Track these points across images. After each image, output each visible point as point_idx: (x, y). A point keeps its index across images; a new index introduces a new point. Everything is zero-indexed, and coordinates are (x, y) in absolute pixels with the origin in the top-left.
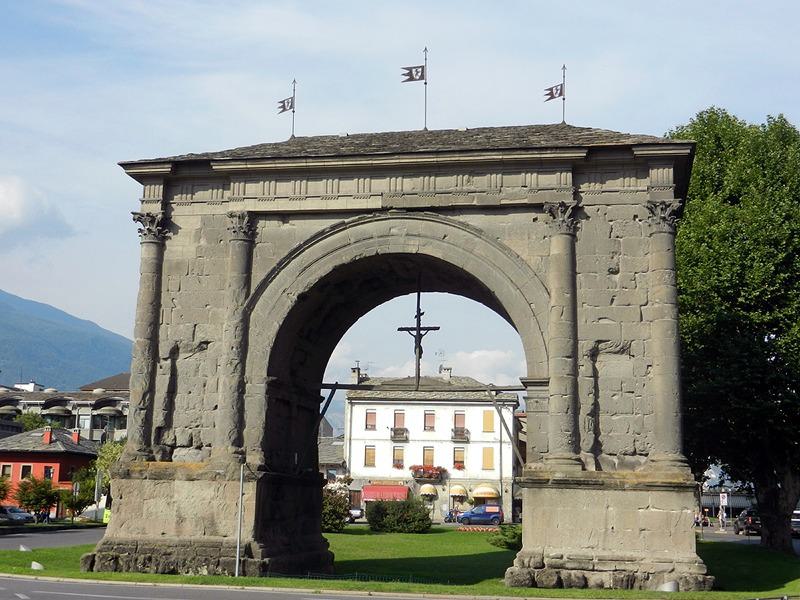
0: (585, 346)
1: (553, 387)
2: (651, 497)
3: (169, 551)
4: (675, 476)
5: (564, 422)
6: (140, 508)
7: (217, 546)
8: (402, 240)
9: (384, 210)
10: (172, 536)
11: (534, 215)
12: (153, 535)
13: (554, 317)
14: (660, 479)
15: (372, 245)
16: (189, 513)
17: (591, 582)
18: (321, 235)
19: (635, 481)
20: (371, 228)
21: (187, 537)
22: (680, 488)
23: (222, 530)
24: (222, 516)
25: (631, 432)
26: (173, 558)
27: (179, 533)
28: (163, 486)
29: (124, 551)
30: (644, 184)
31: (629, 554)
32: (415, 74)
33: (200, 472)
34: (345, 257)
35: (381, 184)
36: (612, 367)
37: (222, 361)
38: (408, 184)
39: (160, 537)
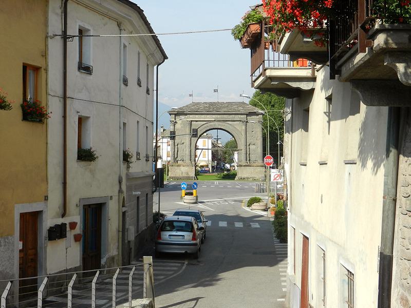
0: (248, 144)
5: (245, 156)
10: (181, 175)
12: (178, 175)
13: (243, 139)
16: (183, 171)
20: (212, 123)
28: (179, 168)
30: (258, 117)
32: (216, 91)
35: (214, 116)
36: (252, 147)
37: (187, 146)
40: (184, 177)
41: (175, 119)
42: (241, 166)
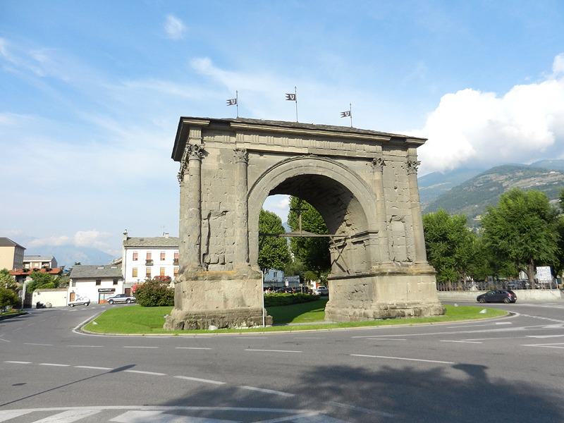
1: (381, 234)
2: (422, 277)
6: (204, 295)
7: (247, 311)
8: (315, 168)
9: (308, 154)
10: (222, 308)
11: (366, 162)
12: (212, 308)
14: (425, 271)
15: (302, 170)
16: (230, 296)
17: (406, 314)
18: (280, 163)
19: (416, 272)
20: (301, 162)
21: (230, 308)
23: (248, 304)
24: (247, 296)
26: (226, 319)
28: (215, 283)
29: (199, 318)
31: (416, 301)
34: (291, 175)
38: (317, 143)
39: (216, 309)
40: (231, 312)
41: (202, 142)
42: (383, 274)
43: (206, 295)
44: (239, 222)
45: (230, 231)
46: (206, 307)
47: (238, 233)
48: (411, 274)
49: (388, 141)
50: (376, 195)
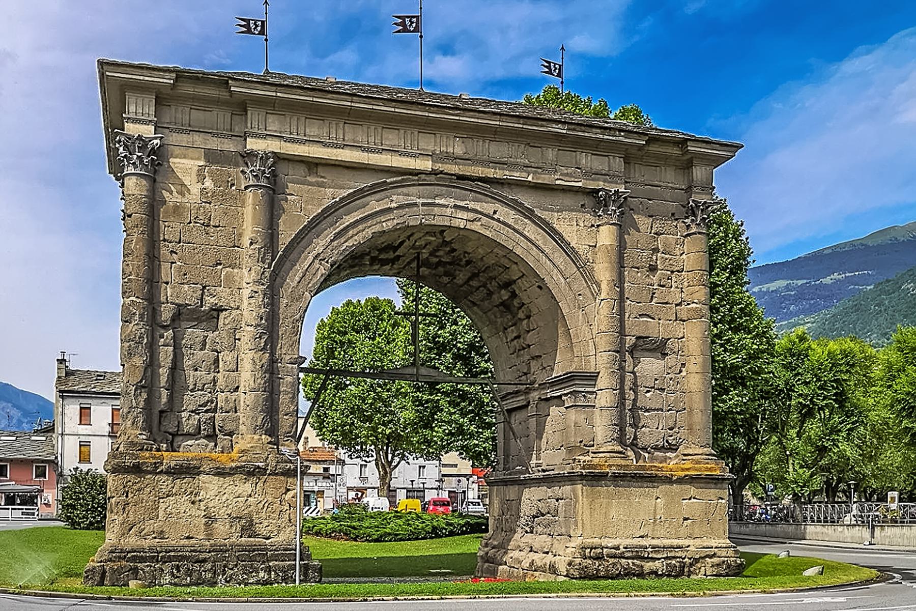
3: (202, 556)
4: (710, 469)
8: (449, 211)
12: (174, 540)
22: (714, 481)
23: (262, 529)
25: (660, 428)
27: (209, 536)
33: (233, 465)
39: (186, 542)
43: (162, 506)
44: (247, 334)
45: (226, 357)
46: (161, 534)
47: (246, 367)
48: (669, 480)
49: (640, 148)
50: (599, 286)
